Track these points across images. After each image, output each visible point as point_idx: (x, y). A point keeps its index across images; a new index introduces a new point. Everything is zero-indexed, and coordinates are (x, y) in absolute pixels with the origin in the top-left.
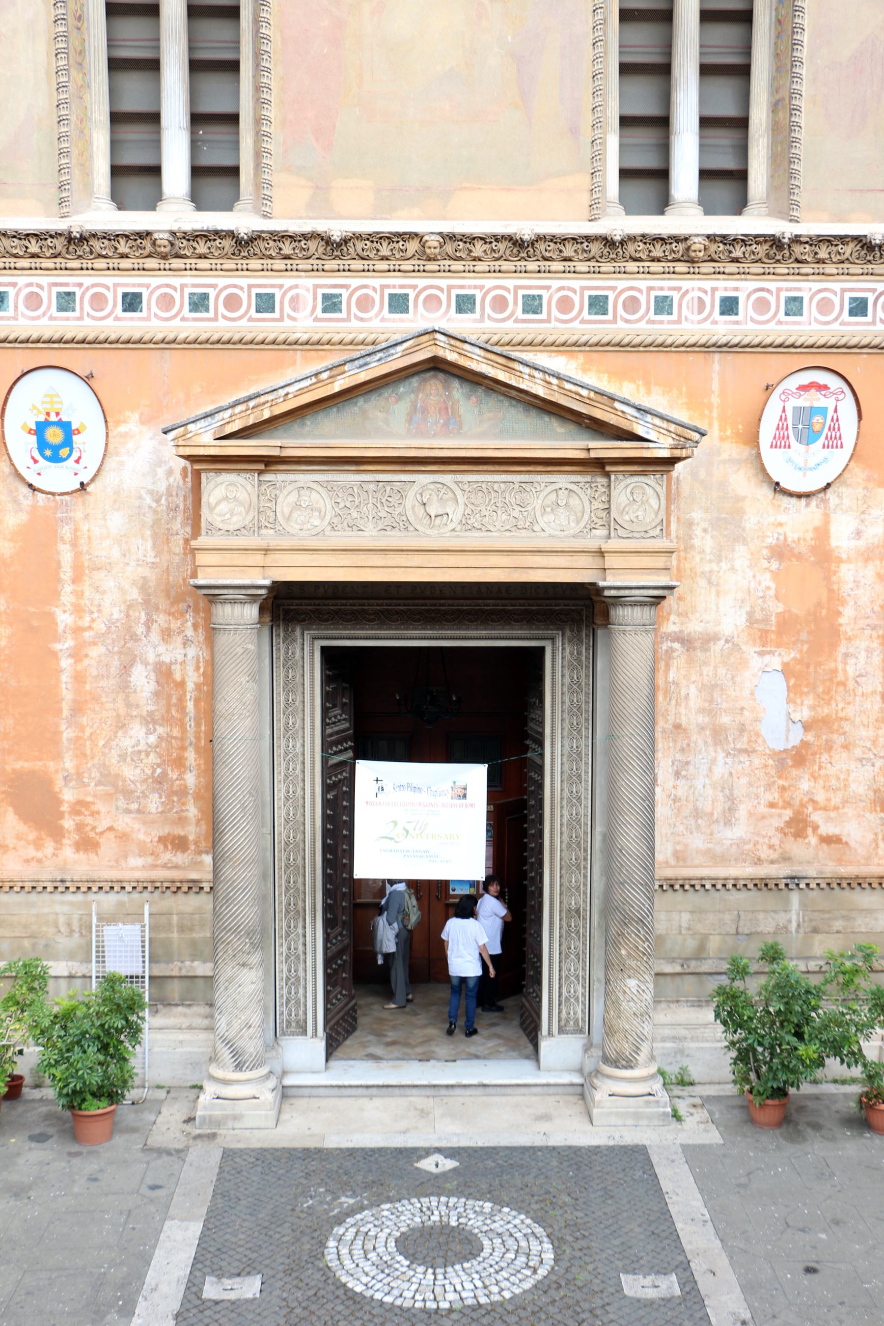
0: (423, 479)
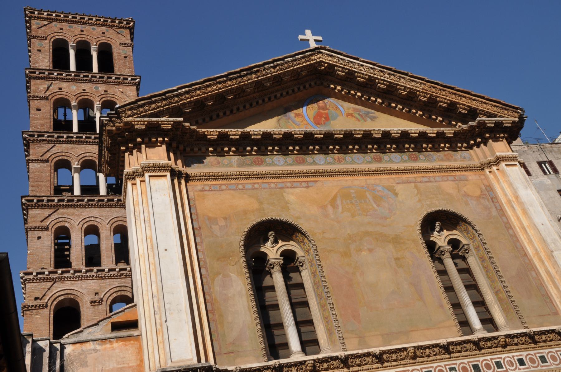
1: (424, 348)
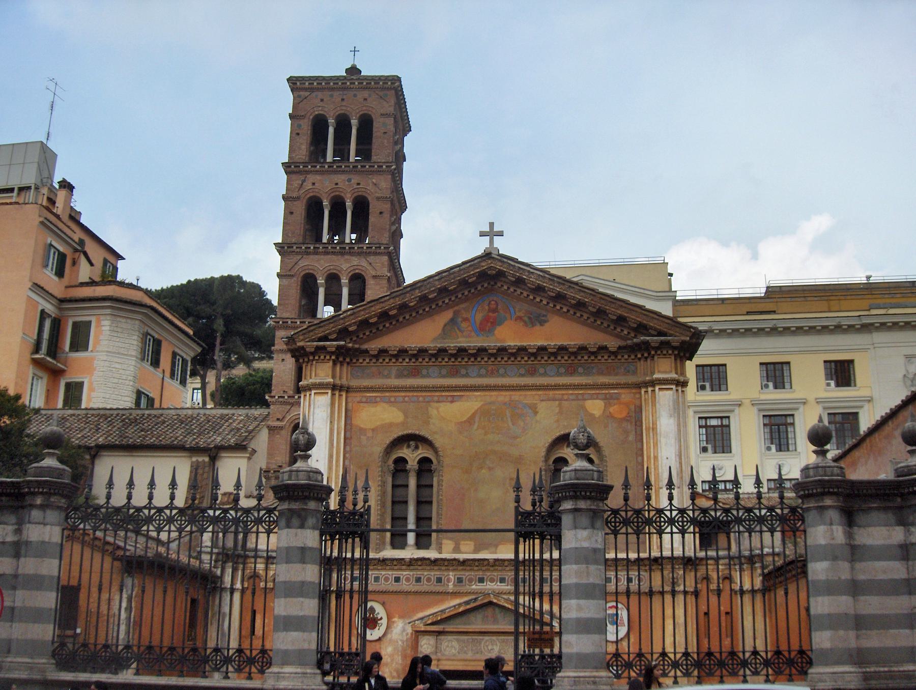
0: (487, 638)
1: (504, 560)
